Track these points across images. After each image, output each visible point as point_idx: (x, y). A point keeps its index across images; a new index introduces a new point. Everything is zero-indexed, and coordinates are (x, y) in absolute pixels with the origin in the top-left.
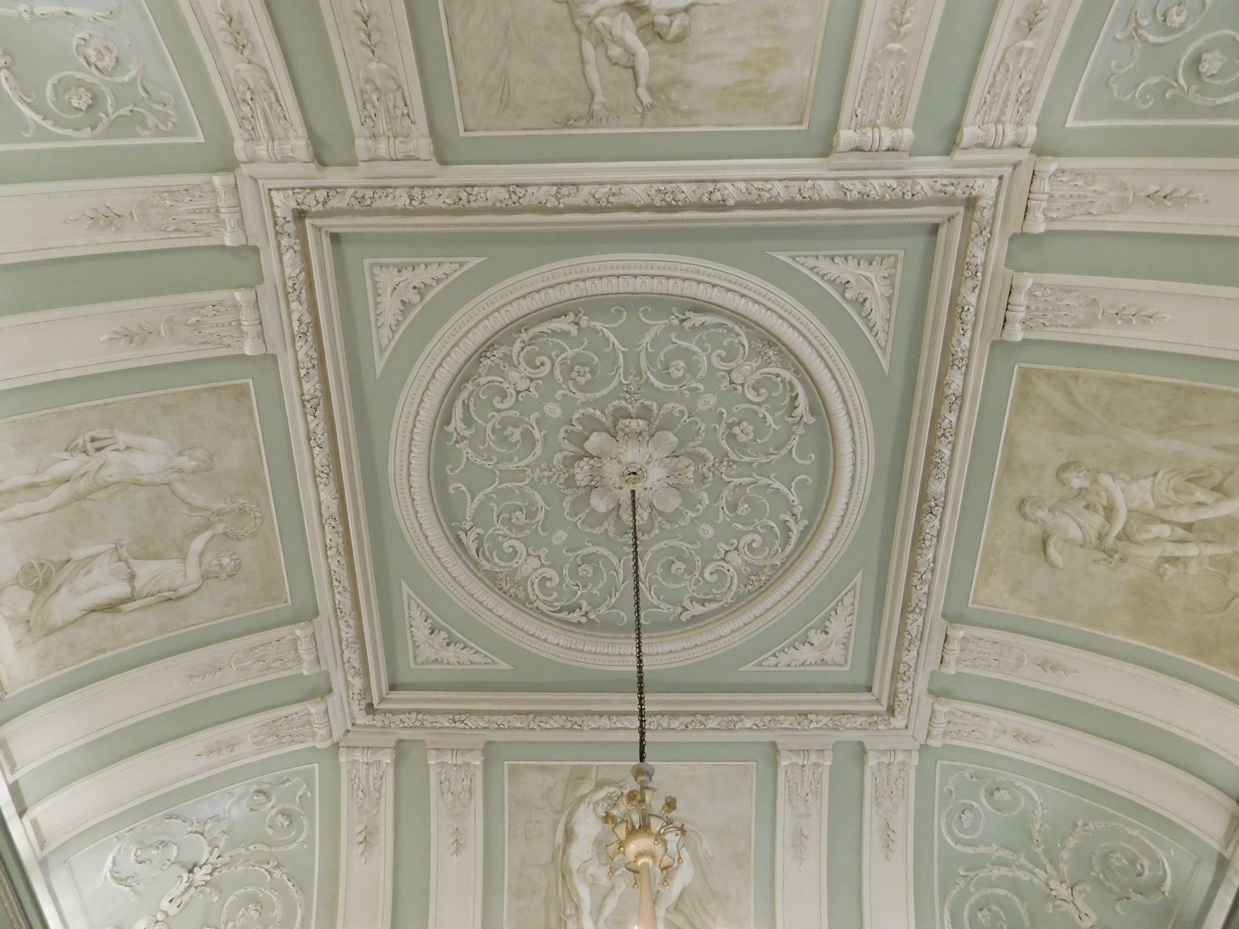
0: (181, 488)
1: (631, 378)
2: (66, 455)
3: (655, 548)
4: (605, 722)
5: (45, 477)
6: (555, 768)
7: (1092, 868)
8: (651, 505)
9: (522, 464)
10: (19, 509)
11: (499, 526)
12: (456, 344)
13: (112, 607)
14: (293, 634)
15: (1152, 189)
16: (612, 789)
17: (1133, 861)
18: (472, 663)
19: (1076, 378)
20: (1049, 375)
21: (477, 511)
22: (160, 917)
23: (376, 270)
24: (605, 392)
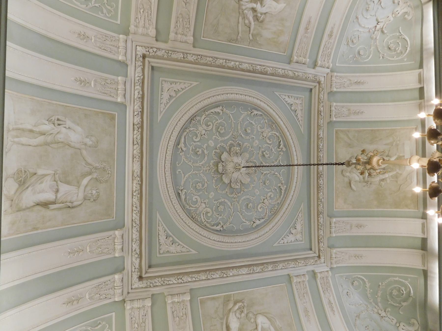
0: (84, 152)
1: (235, 133)
2: (47, 122)
3: (242, 199)
4: (235, 272)
5: (36, 129)
6: (218, 297)
7: (388, 301)
8: (241, 181)
9: (201, 164)
10: (24, 140)
11: (192, 189)
12: (186, 113)
13: (45, 205)
14: (114, 234)
15: (356, 81)
16: (240, 304)
17: (399, 290)
18: (182, 252)
19: (349, 131)
20: (342, 131)
21: (185, 182)
23: (163, 82)
24: (228, 137)
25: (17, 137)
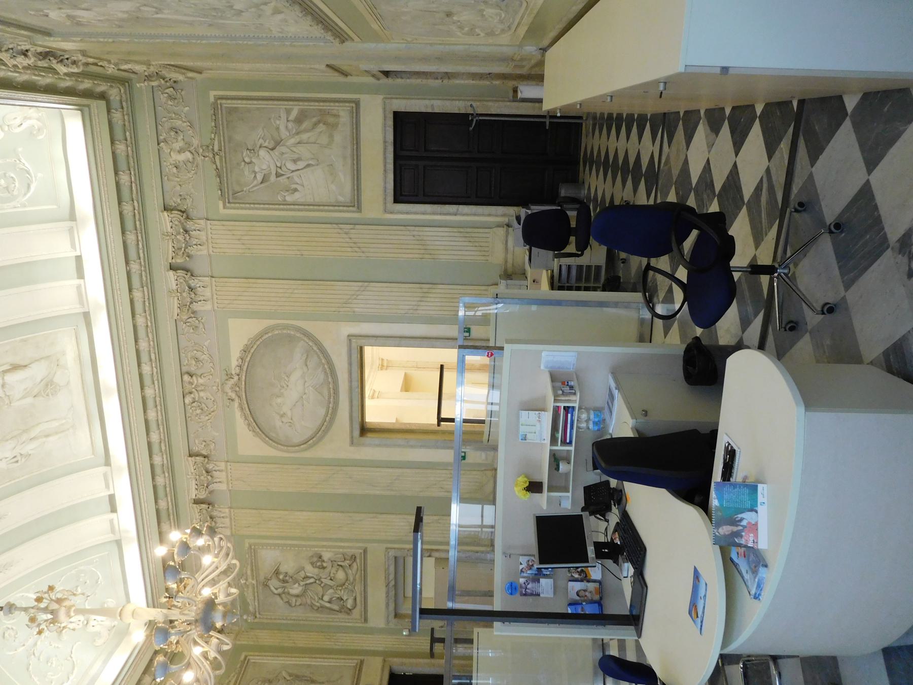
10: (55, 424)
13: (15, 367)
22: (6, 128)
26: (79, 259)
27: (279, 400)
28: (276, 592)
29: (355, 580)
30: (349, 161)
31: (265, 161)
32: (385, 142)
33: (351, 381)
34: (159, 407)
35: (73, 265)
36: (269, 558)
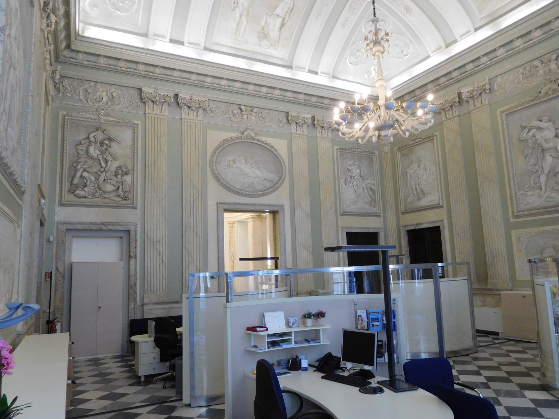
2: (235, 12)
10: (242, 30)
13: (283, 25)
25: (240, 34)
26: (316, 73)
27: (243, 161)
28: (91, 136)
29: (105, 198)
30: (358, 211)
31: (356, 171)
32: (369, 228)
33: (259, 205)
34: (240, 90)
35: (315, 70)
36: (126, 136)
